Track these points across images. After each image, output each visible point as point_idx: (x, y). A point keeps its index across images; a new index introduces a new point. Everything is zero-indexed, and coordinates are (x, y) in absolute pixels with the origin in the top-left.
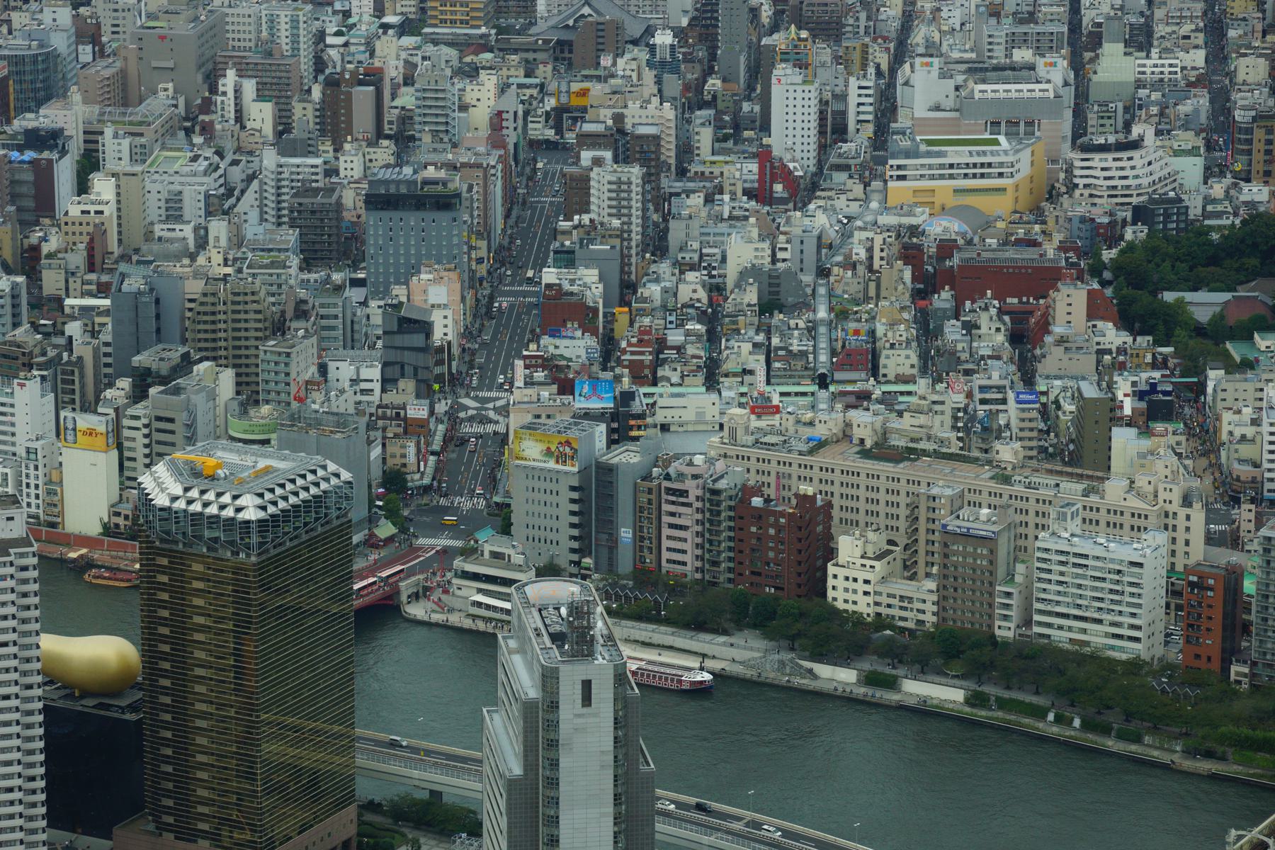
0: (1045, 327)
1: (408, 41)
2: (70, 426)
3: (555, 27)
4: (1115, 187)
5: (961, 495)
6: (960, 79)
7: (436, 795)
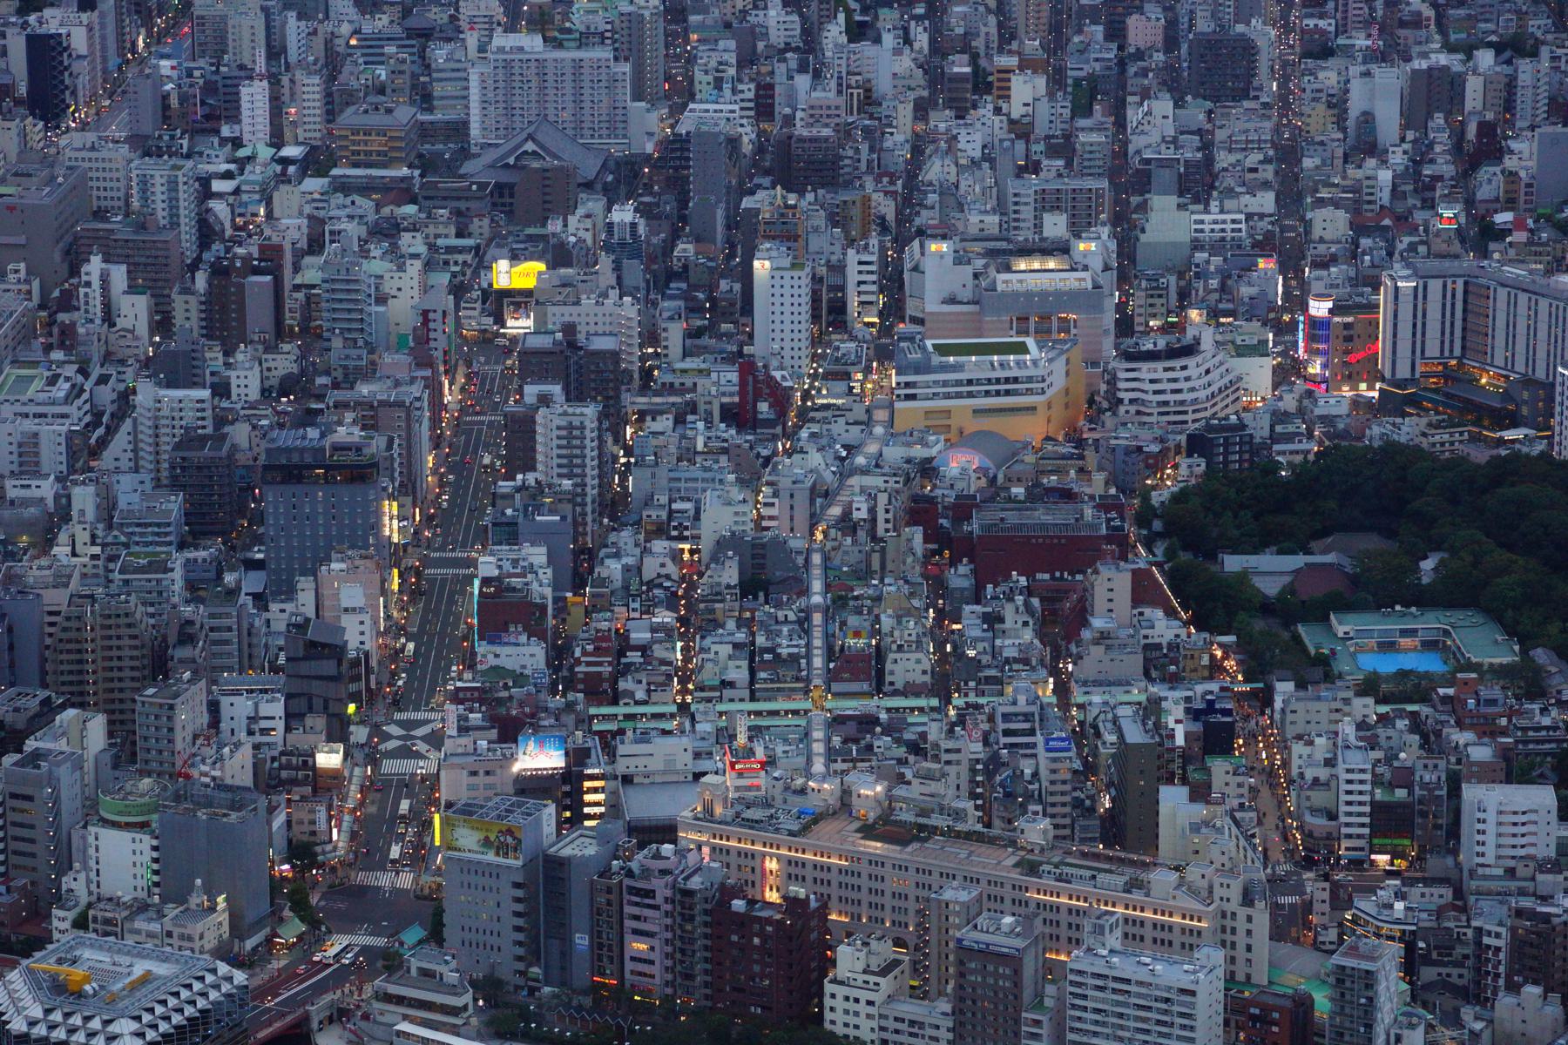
0: (1081, 615)
1: (313, 184)
3: (492, 166)
4: (1166, 403)
5: (979, 899)
6: (979, 263)
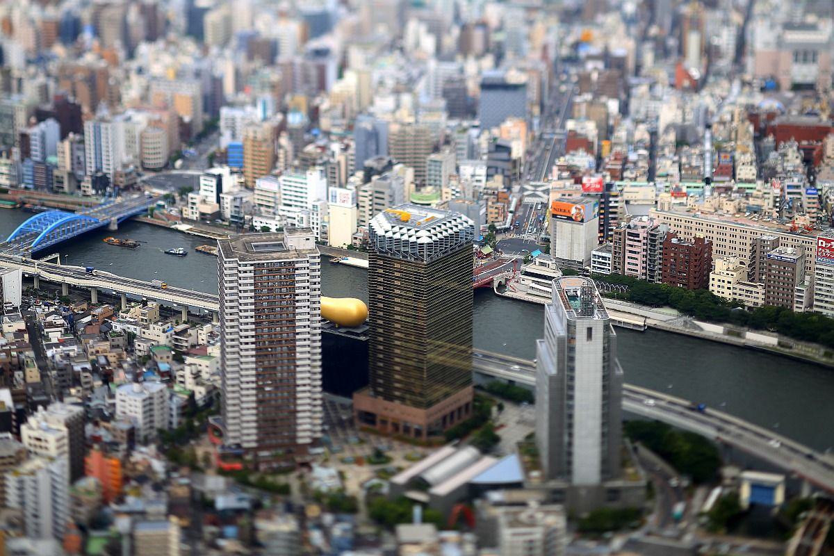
7: (511, 382)
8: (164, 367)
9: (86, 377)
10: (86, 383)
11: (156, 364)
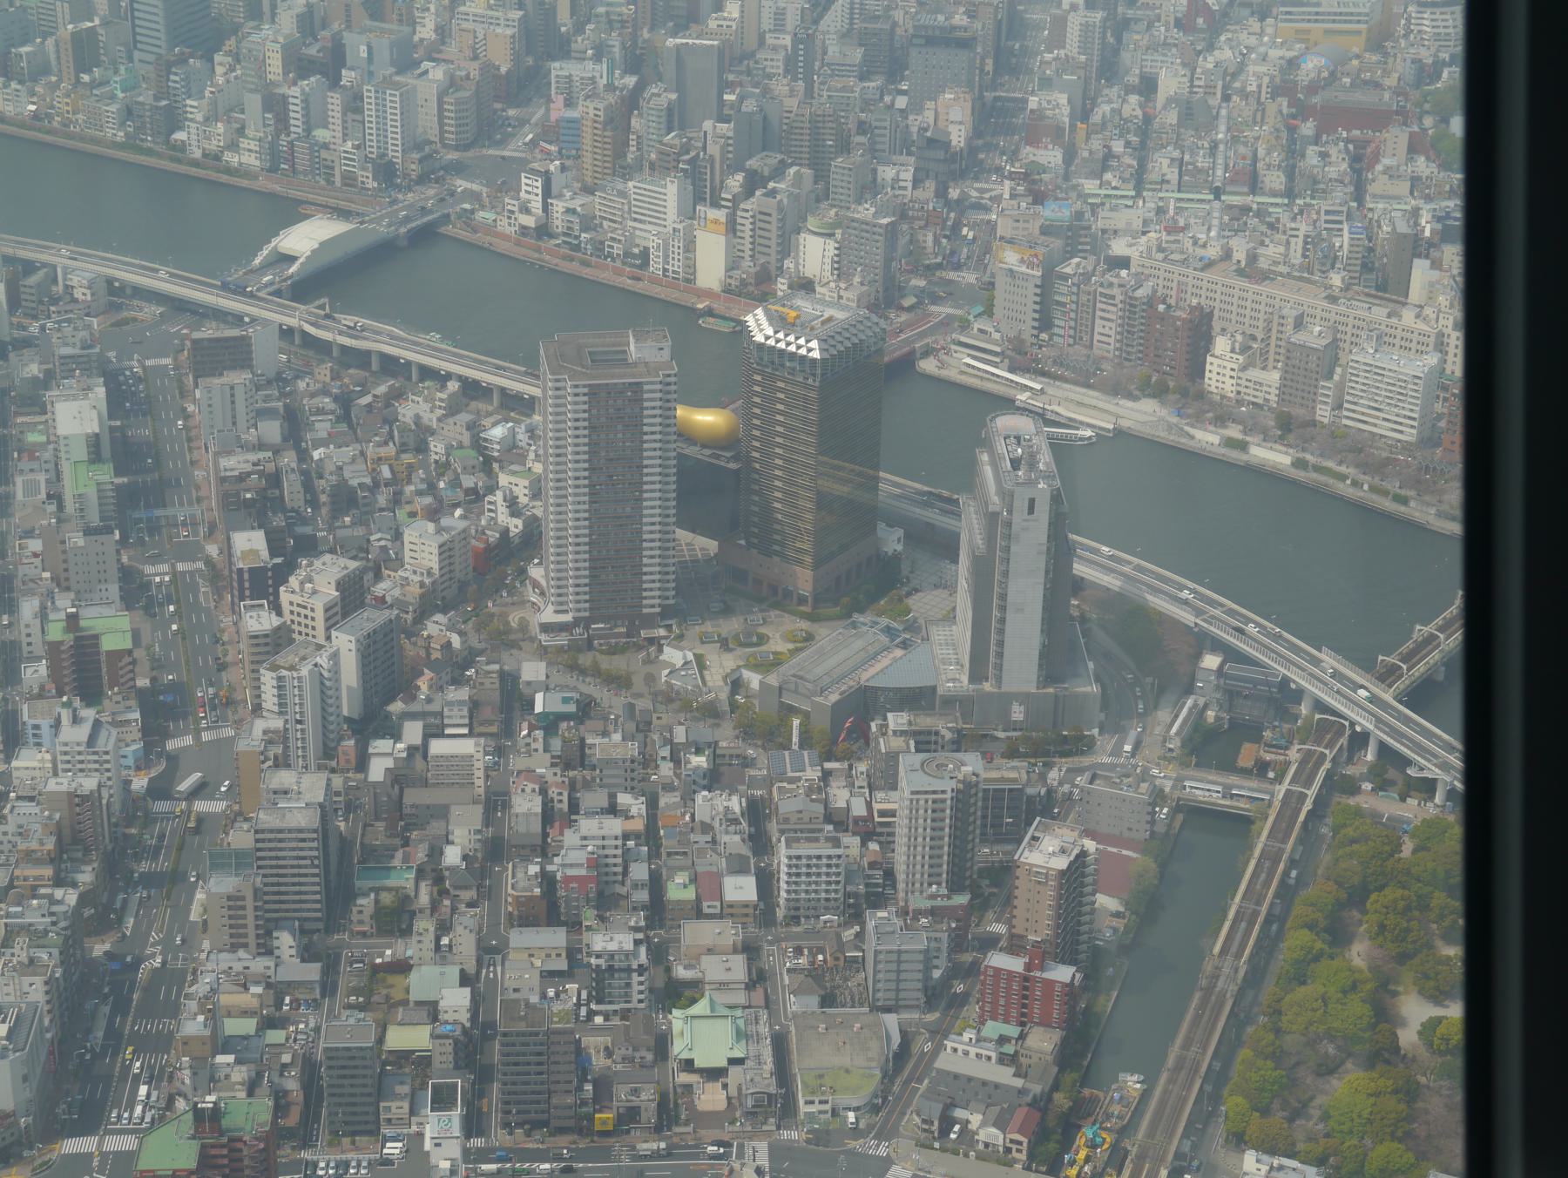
0: (1376, 158)
2: (703, 216)
4: (1439, 34)
7: (930, 526)
8: (468, 481)
9: (365, 497)
10: (365, 505)
11: (457, 478)
